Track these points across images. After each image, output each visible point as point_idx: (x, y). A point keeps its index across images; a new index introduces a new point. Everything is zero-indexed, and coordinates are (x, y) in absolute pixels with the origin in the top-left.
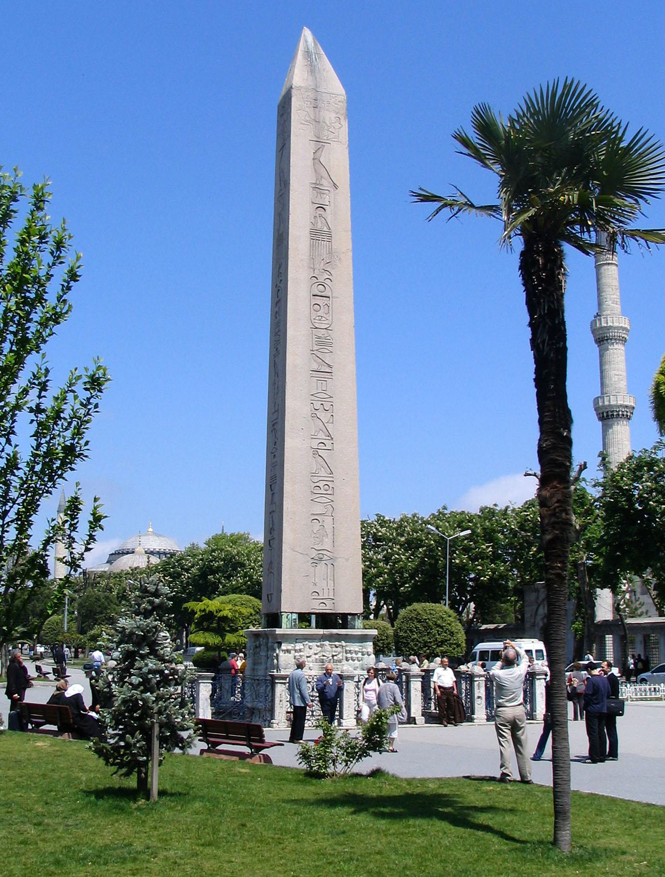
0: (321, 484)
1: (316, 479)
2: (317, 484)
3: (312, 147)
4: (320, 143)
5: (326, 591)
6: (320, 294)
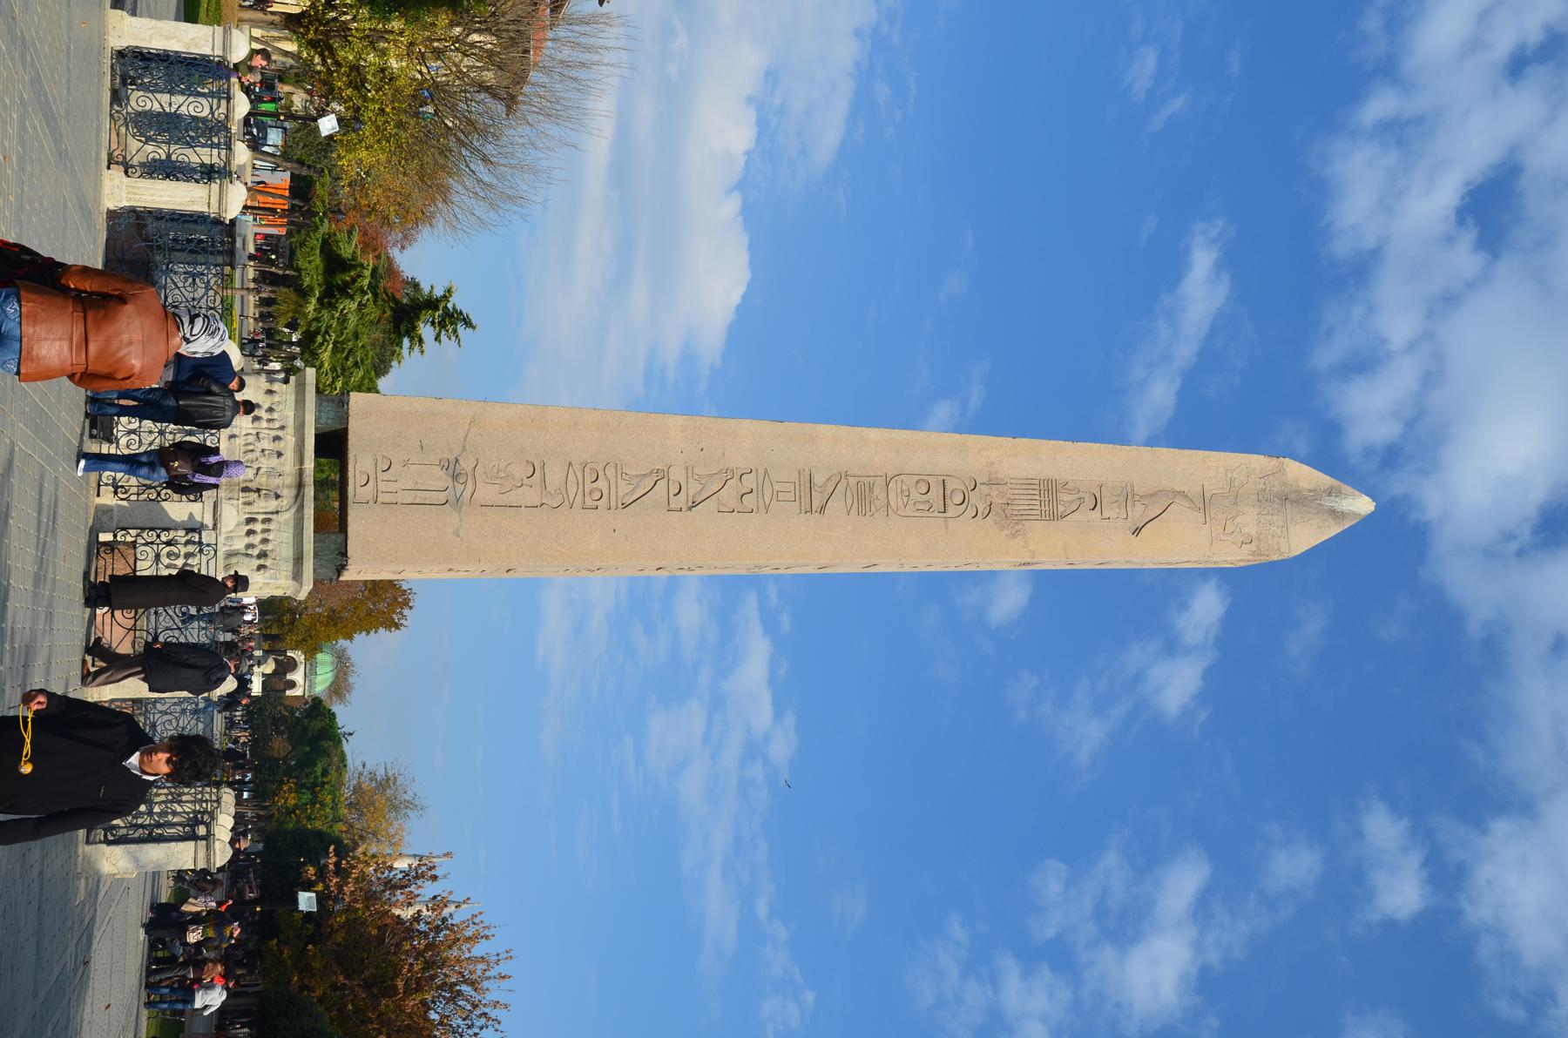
0: (600, 484)
4: (1204, 503)
5: (392, 487)
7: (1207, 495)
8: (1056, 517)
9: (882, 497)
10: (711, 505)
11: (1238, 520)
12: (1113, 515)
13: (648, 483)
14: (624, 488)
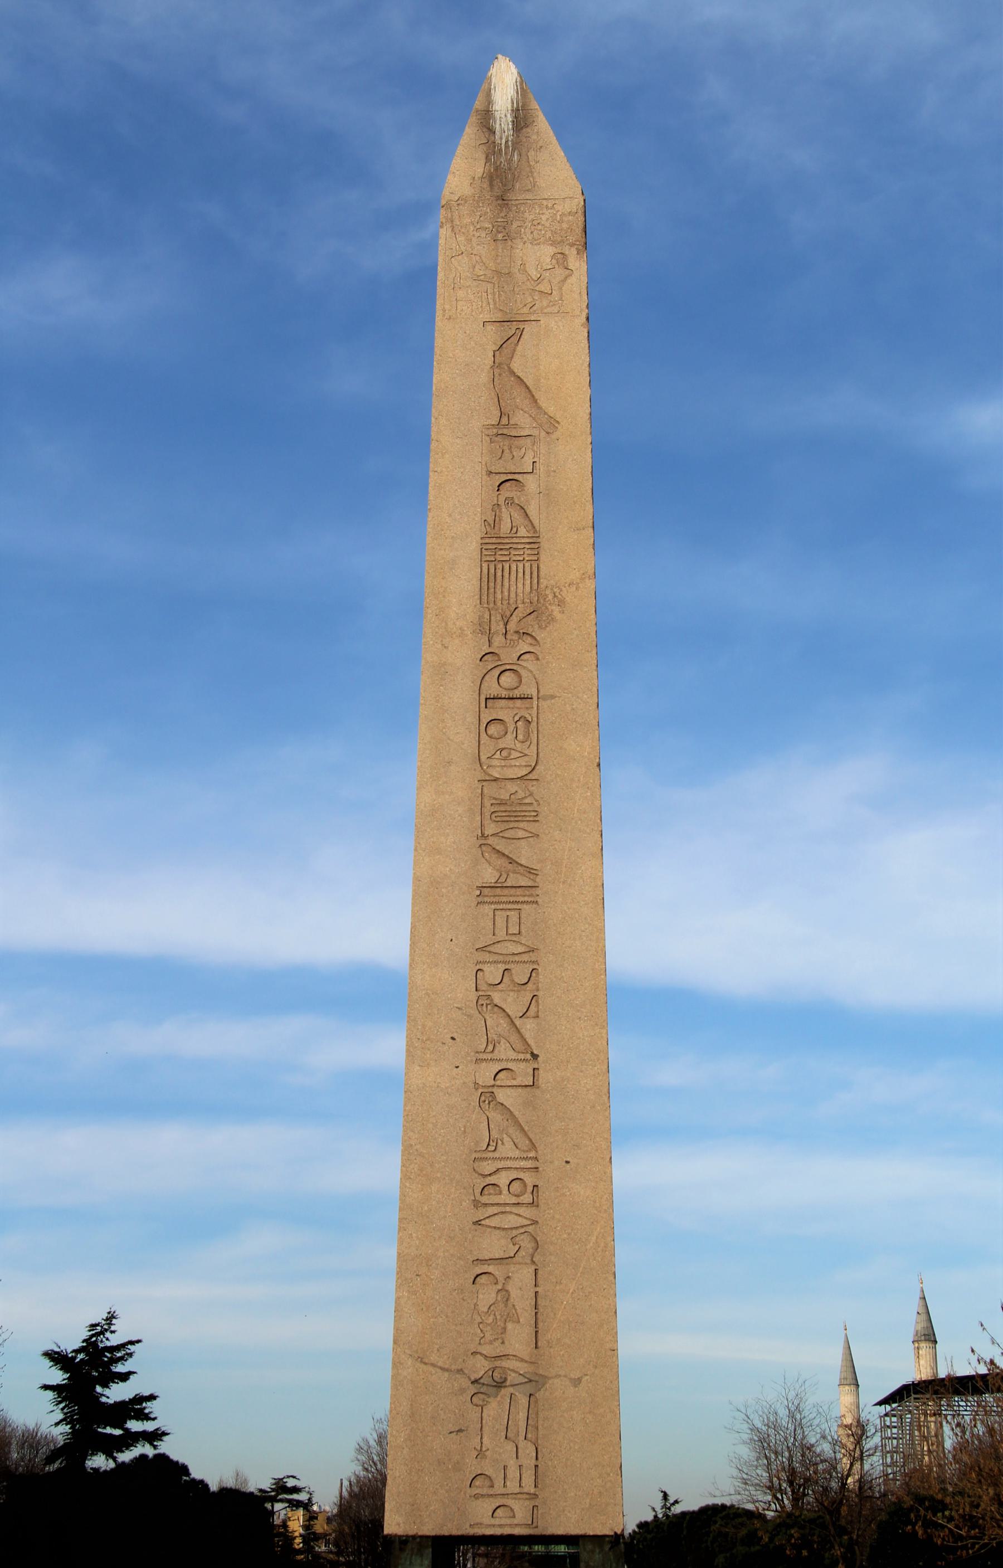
0: (503, 1179)
1: (488, 1167)
4: (511, 330)
5: (513, 1473)
6: (504, 693)
7: (499, 316)
8: (534, 543)
9: (512, 787)
10: (528, 1027)
11: (534, 274)
12: (528, 460)
13: (496, 1116)
14: (507, 1149)
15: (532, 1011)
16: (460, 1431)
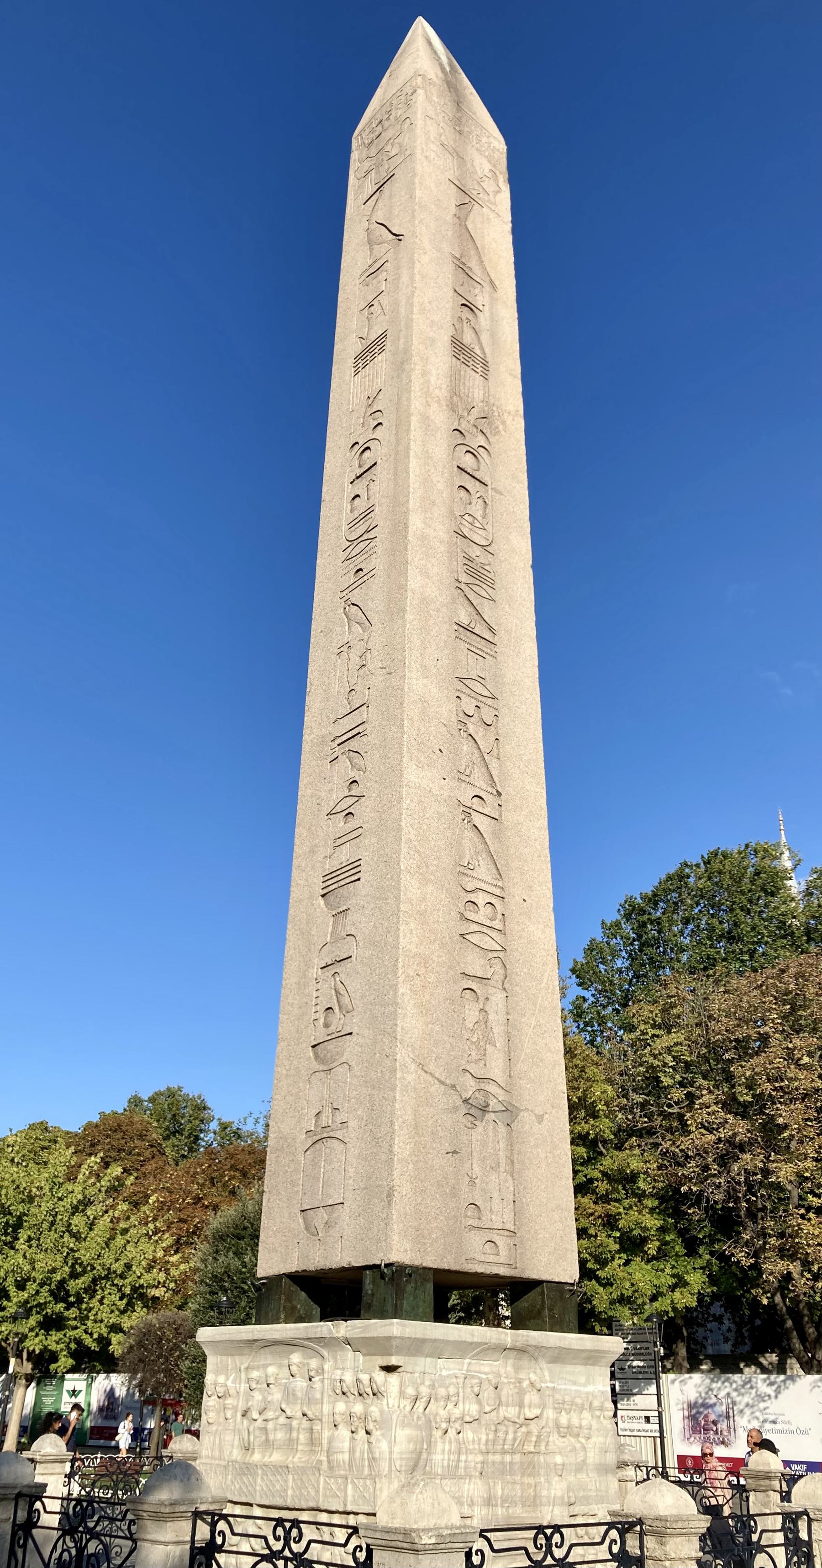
0: (481, 899)
2: (472, 897)
3: (452, 198)
15: (495, 752)
16: (455, 1152)
